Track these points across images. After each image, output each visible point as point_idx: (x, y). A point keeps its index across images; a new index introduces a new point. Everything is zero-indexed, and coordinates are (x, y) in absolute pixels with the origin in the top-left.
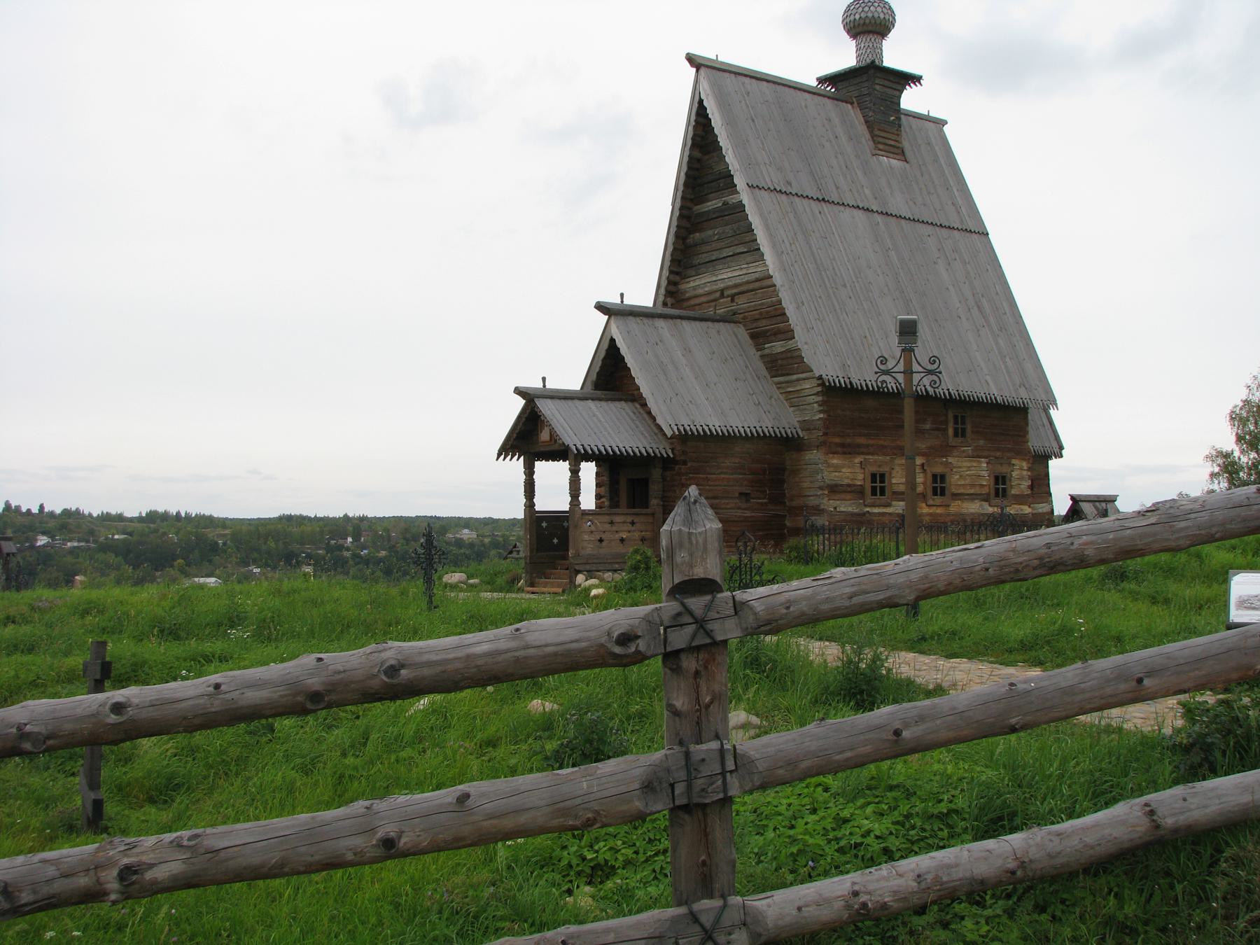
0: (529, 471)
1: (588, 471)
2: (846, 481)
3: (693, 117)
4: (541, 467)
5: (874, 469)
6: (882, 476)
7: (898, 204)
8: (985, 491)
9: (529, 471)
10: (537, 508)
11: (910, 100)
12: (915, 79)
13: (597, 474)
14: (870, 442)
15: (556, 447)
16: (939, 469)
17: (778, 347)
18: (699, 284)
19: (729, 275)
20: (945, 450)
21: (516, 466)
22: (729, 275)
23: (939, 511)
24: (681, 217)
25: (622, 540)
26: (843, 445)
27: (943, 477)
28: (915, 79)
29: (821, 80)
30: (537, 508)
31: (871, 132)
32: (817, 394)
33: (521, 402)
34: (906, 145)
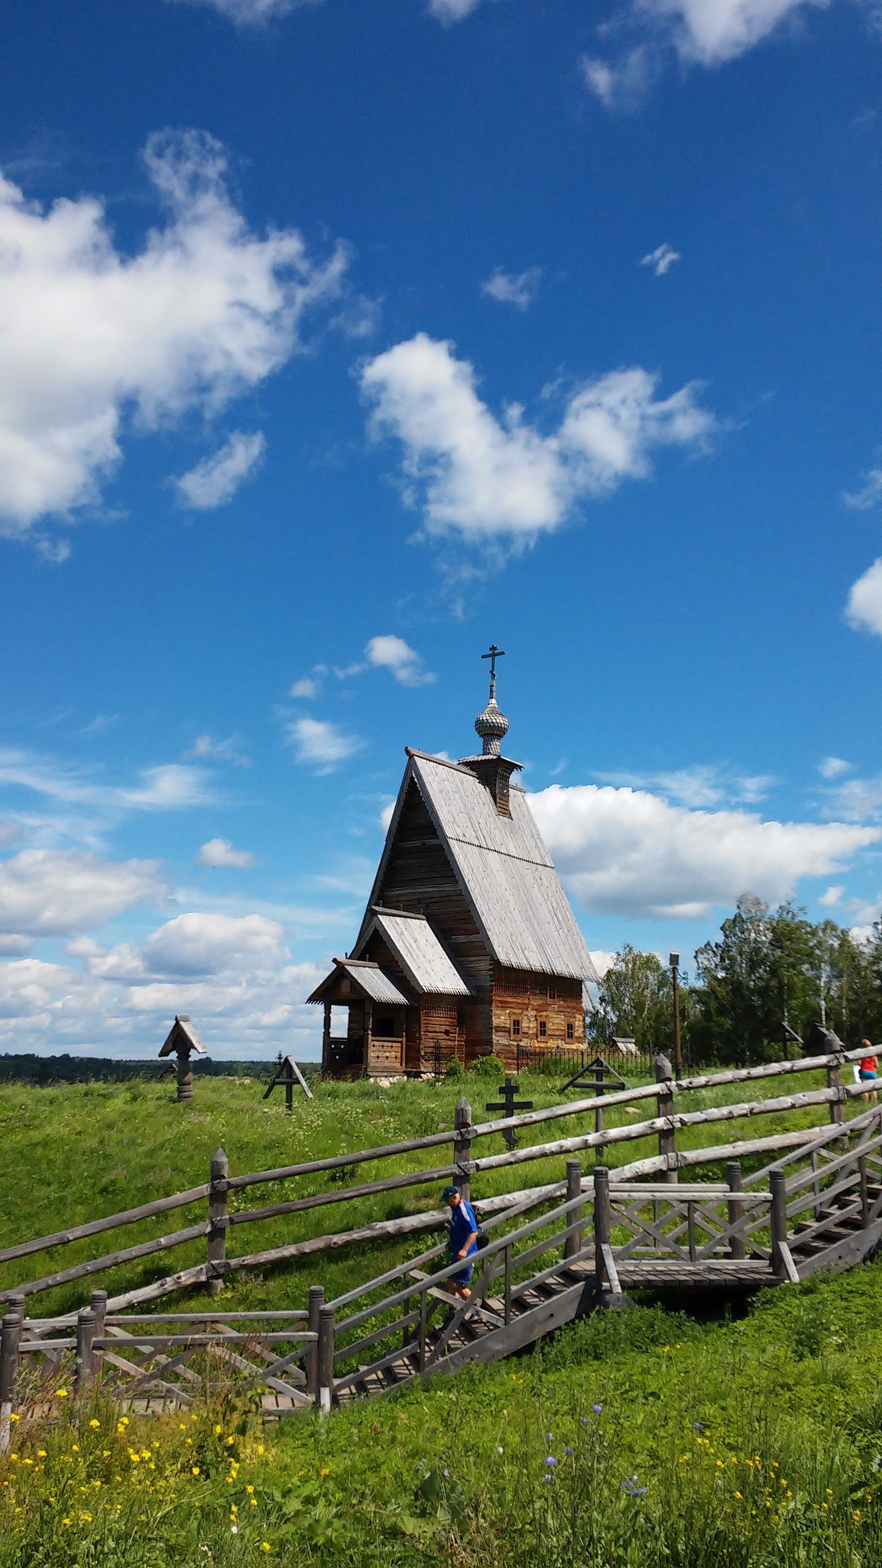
0: (328, 1012)
2: (503, 1025)
3: (406, 787)
4: (334, 1008)
5: (513, 1017)
6: (518, 1021)
8: (562, 1033)
9: (328, 1012)
10: (331, 1036)
13: (350, 1014)
14: (514, 1000)
15: (354, 997)
17: (462, 939)
21: (320, 1008)
23: (543, 1045)
24: (392, 850)
25: (387, 1057)
26: (501, 1002)
30: (331, 1036)
31: (495, 800)
32: (490, 970)
34: (511, 808)
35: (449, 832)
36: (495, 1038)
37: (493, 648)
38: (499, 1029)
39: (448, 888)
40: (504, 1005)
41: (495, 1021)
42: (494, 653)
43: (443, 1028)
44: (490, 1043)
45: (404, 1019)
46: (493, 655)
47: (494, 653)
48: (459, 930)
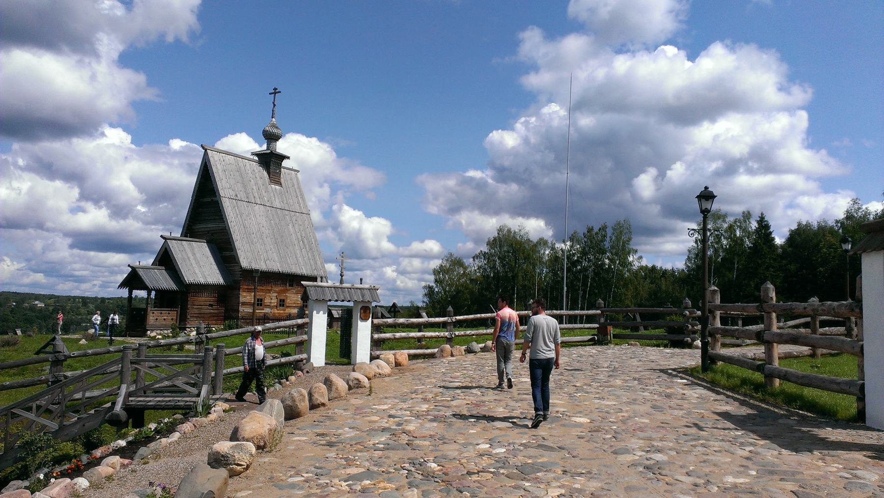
1: (153, 293)
7: (277, 204)
11: (285, 163)
12: (288, 158)
16: (282, 298)
17: (227, 253)
18: (201, 227)
19: (211, 226)
20: (286, 291)
22: (211, 226)
27: (284, 301)
28: (288, 158)
29: (253, 154)
33: (130, 269)
34: (282, 181)
35: (222, 193)
36: (241, 309)
37: (275, 89)
38: (244, 304)
39: (221, 225)
40: (249, 291)
41: (242, 299)
42: (275, 92)
43: (208, 303)
44: (238, 311)
45: (179, 298)
46: (275, 93)
47: (275, 92)
48: (223, 250)
